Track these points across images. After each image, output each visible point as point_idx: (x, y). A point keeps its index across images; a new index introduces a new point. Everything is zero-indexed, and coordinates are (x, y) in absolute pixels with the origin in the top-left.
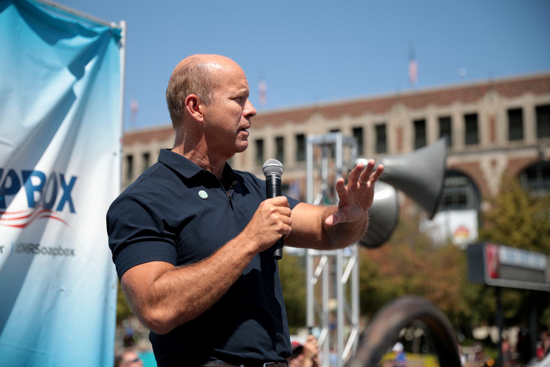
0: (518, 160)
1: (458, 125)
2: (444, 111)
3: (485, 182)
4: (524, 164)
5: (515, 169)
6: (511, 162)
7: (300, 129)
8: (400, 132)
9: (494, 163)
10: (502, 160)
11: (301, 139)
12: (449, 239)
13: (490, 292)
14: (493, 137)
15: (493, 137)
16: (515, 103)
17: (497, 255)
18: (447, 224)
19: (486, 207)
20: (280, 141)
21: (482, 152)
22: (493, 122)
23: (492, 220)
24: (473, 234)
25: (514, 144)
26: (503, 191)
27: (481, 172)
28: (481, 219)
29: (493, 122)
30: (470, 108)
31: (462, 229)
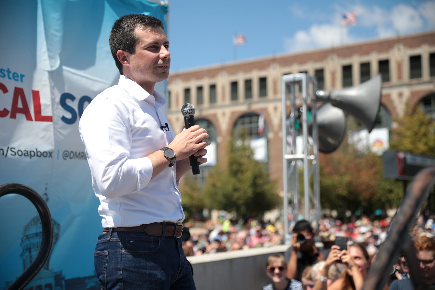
0: (418, 92)
1: (375, 67)
2: (365, 59)
3: (395, 108)
4: (422, 95)
5: (416, 99)
6: (413, 94)
7: (263, 74)
8: (333, 74)
9: (400, 95)
10: (406, 92)
11: (263, 81)
12: (368, 148)
13: (401, 184)
14: (400, 76)
15: (400, 76)
16: (416, 52)
17: (405, 159)
18: (367, 138)
19: (395, 125)
20: (248, 83)
21: (392, 87)
22: (399, 66)
23: (400, 134)
24: (386, 145)
25: (415, 81)
26: (406, 114)
27: (391, 102)
28: (391, 133)
29: (399, 66)
30: (383, 56)
31: (379, 142)
